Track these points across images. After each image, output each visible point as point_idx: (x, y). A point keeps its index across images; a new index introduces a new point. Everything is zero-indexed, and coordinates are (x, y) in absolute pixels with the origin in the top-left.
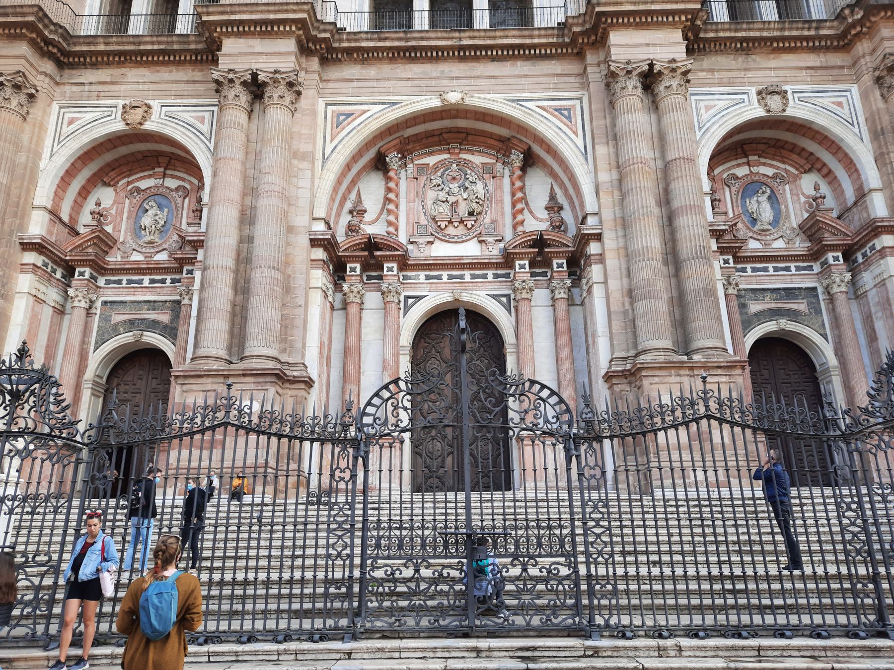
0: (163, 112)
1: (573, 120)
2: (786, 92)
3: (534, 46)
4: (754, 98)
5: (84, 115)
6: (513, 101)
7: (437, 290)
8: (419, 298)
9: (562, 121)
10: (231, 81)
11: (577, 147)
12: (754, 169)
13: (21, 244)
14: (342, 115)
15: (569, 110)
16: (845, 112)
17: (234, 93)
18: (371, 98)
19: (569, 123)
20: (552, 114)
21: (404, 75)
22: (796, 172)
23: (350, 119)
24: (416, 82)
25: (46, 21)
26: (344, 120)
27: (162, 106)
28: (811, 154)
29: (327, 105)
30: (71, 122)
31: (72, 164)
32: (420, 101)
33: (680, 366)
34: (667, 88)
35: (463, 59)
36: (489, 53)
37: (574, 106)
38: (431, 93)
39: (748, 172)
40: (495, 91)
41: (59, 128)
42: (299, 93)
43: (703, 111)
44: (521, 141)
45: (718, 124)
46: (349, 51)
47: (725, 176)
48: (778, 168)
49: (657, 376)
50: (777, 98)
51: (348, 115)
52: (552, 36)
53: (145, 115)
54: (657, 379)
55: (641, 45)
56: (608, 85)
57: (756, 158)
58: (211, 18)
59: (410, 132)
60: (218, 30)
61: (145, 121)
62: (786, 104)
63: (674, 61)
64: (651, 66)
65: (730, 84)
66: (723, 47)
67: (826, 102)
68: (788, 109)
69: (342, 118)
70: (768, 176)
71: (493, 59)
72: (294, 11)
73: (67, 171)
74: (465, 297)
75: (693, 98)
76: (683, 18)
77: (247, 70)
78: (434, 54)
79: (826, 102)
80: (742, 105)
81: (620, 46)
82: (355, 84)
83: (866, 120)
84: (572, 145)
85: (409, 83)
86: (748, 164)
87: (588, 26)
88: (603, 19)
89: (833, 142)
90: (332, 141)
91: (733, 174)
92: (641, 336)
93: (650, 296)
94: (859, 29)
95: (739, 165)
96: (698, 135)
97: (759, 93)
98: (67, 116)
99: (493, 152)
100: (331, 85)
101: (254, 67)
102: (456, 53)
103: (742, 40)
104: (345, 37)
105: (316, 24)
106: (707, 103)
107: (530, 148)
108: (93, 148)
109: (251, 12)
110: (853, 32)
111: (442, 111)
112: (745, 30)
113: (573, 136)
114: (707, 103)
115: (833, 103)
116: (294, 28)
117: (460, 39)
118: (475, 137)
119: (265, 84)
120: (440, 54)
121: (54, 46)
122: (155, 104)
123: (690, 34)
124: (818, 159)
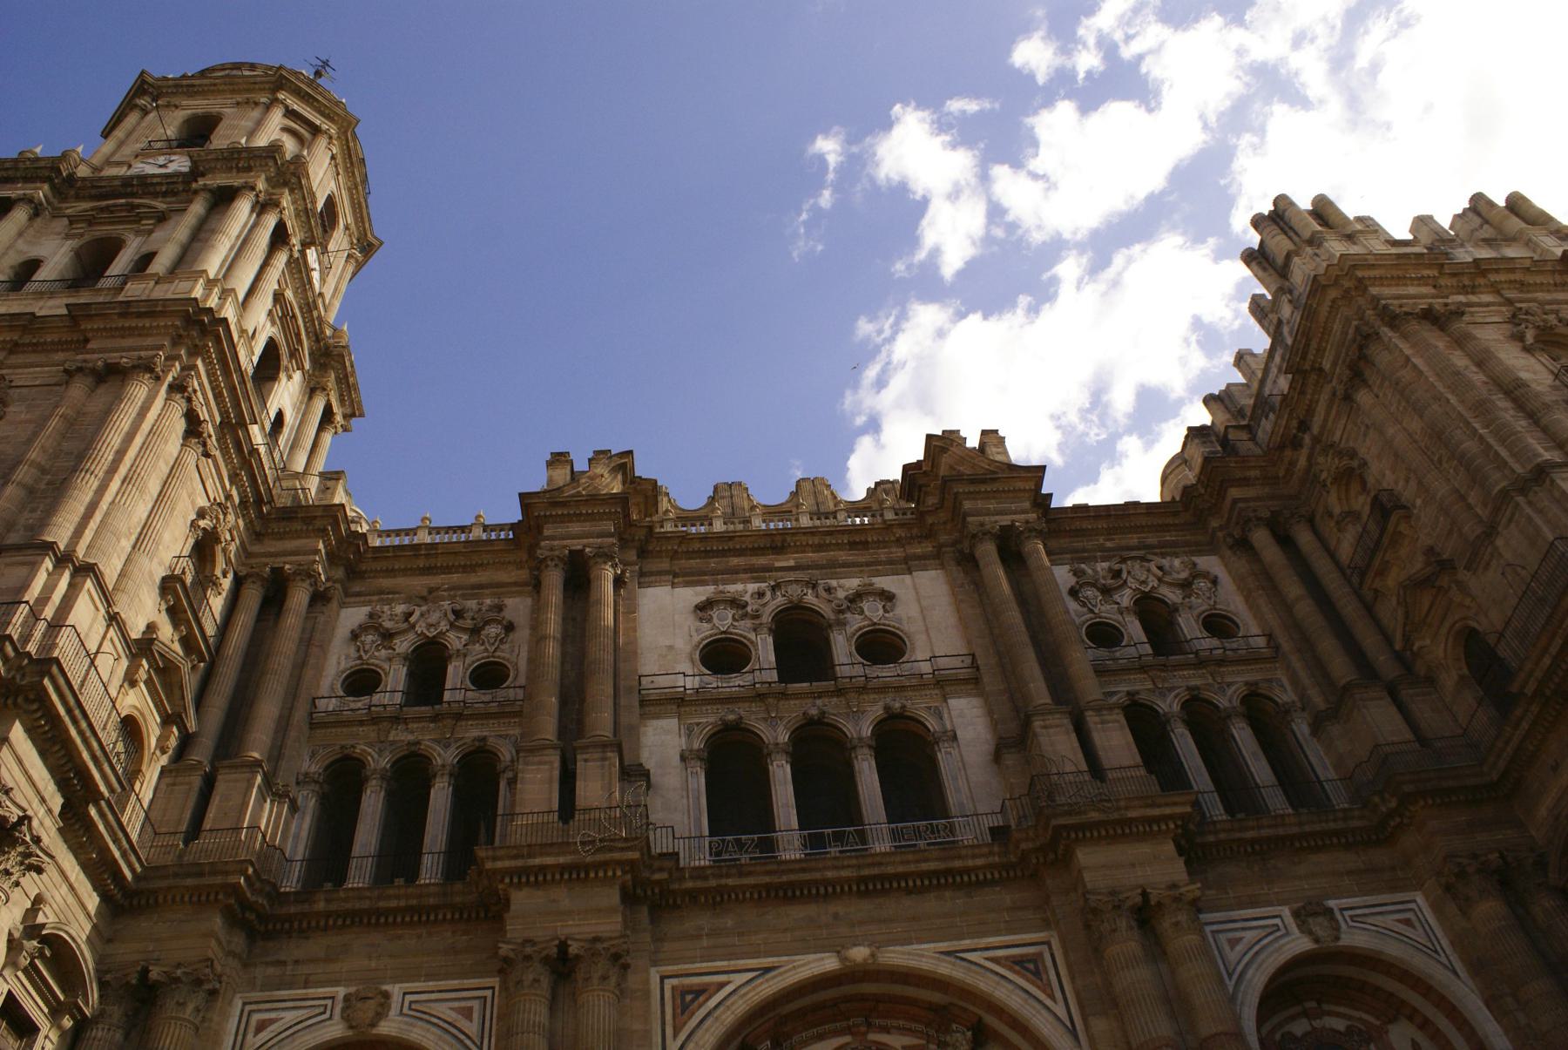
0: (406, 1004)
1: (1044, 977)
2: (1331, 911)
3: (968, 871)
4: (1289, 920)
5: (283, 1014)
6: (948, 953)
9: (1028, 981)
10: (528, 958)
11: (1058, 1019)
12: (1317, 1023)
14: (690, 992)
15: (1036, 959)
16: (1418, 935)
17: (531, 977)
18: (732, 962)
19: (1039, 983)
20: (1010, 969)
22: (1378, 1023)
23: (701, 999)
26: (693, 1001)
27: (405, 994)
28: (1392, 995)
29: (662, 978)
30: (262, 1026)
32: (809, 963)
34: (1177, 924)
35: (865, 894)
36: (903, 884)
37: (1040, 955)
38: (822, 949)
39: (1309, 1028)
40: (920, 941)
41: (240, 1038)
42: (626, 967)
43: (1227, 948)
44: (965, 1010)
45: (1255, 966)
46: (693, 895)
47: (1278, 1036)
48: (1350, 1018)
50: (1320, 919)
51: (701, 992)
52: (991, 853)
53: (380, 1010)
56: (1088, 927)
57: (1313, 1004)
58: (499, 864)
60: (507, 880)
61: (380, 1019)
62: (1337, 929)
63: (1174, 886)
64: (1144, 894)
65: (1254, 903)
66: (1228, 852)
67: (1389, 920)
68: (1343, 936)
69: (689, 998)
70: (1340, 1033)
71: (909, 892)
72: (622, 849)
75: (1208, 929)
76: (1172, 826)
77: (553, 940)
78: (822, 891)
79: (1389, 920)
80: (1278, 934)
82: (705, 942)
83: (1452, 943)
84: (1051, 1019)
86: (1306, 1014)
88: (1065, 834)
89: (1419, 979)
90: (675, 1036)
91: (1289, 1033)
94: (1398, 820)
95: (1293, 1018)
96: (1230, 985)
97: (1296, 914)
98: (256, 1017)
99: (920, 1027)
101: (562, 932)
102: (855, 888)
103: (1253, 842)
106: (1231, 935)
107: (980, 1019)
109: (558, 855)
110: (1392, 824)
112: (1253, 828)
113: (1049, 1002)
114: (1231, 935)
115: (1399, 921)
116: (619, 873)
119: (577, 957)
120: (830, 889)
122: (396, 990)
123: (1183, 842)
124: (1403, 1002)
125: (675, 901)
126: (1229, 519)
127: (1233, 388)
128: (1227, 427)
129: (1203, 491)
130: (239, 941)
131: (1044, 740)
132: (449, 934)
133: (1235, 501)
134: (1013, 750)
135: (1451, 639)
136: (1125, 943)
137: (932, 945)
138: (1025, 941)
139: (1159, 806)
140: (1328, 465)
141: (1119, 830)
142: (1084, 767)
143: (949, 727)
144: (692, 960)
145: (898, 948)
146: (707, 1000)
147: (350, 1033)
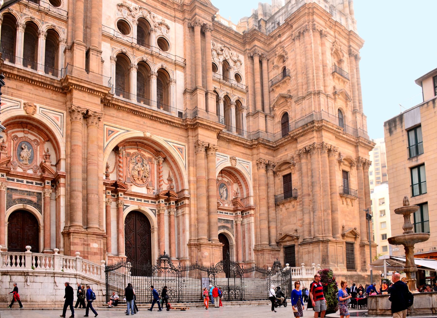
3: (174, 123)
18: (121, 126)
21: (131, 120)
24: (136, 124)
33: (210, 244)
54: (204, 248)
55: (206, 136)
56: (195, 147)
63: (214, 145)
64: (209, 145)
71: (161, 122)
76: (218, 131)
81: (201, 135)
87: (192, 123)
92: (200, 234)
93: (203, 222)
125: (109, 105)
126: (251, 49)
127: (267, 5)
128: (261, 19)
129: (249, 37)
131: (199, 97)
132: (51, 93)
133: (255, 46)
134: (189, 94)
135: (282, 112)
136: (202, 153)
137: (163, 138)
138: (183, 144)
139: (218, 126)
140: (279, 51)
141: (208, 128)
142: (205, 109)
143: (175, 79)
145: (156, 136)
146: (114, 134)
147: (27, 115)
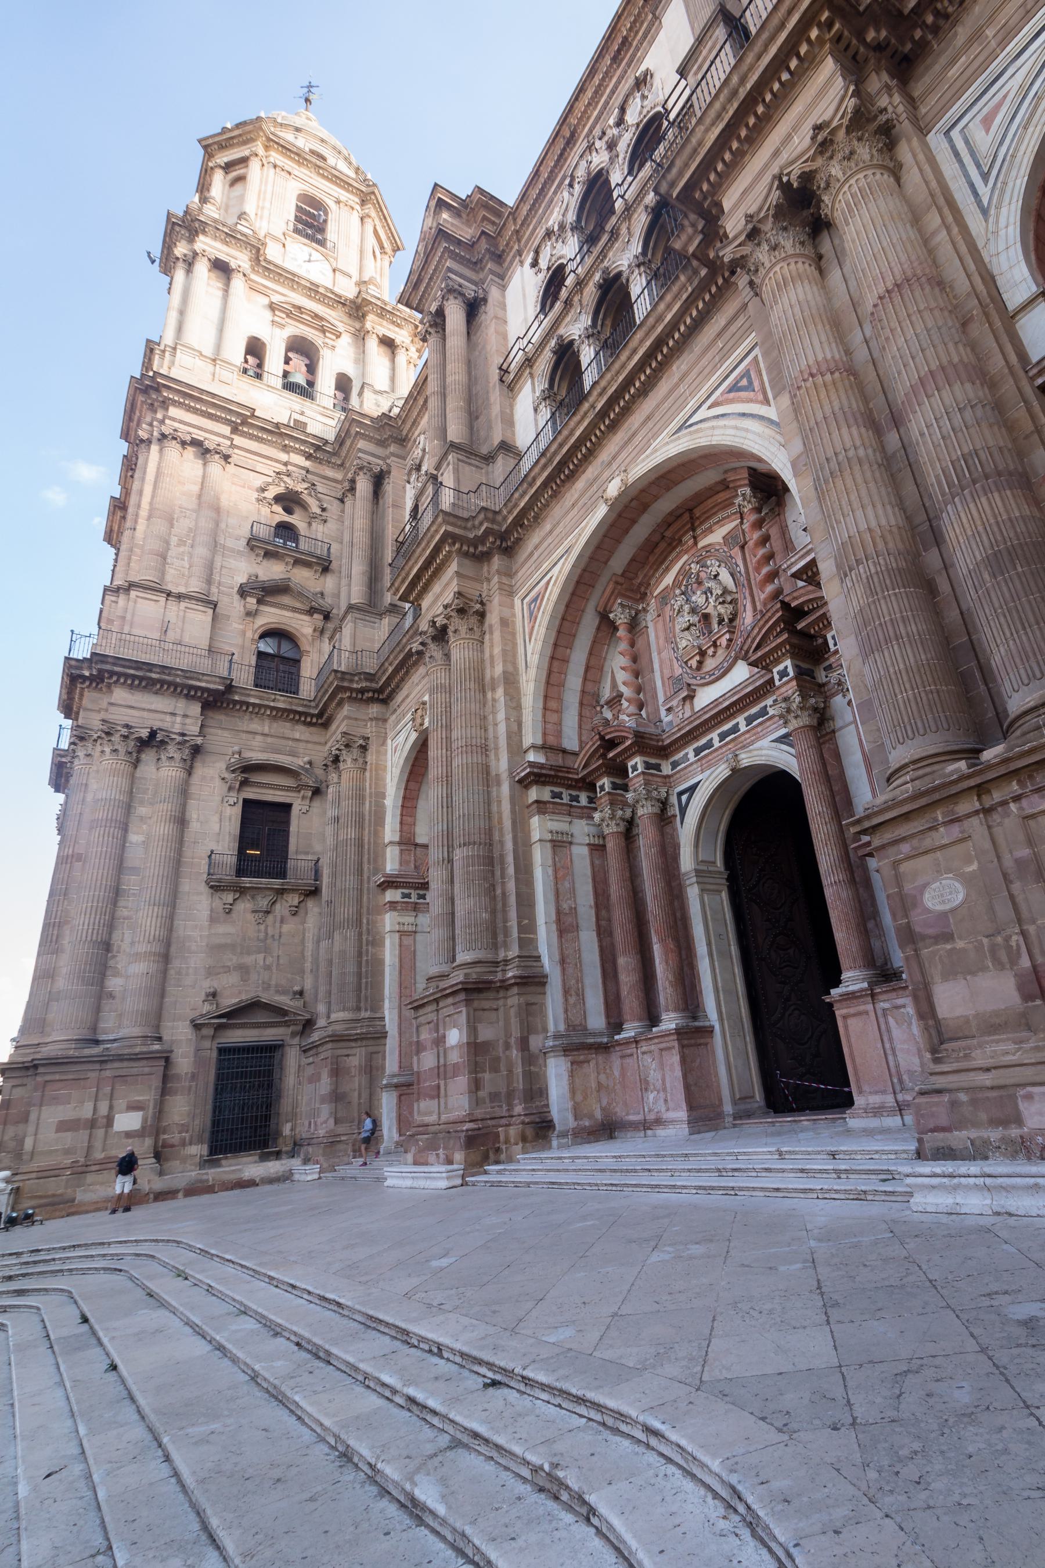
6: (680, 429)
7: (709, 767)
8: (692, 789)
13: (379, 886)
25: (347, 677)
31: (406, 789)
35: (614, 426)
49: (903, 839)
51: (535, 600)
59: (619, 562)
73: (404, 798)
74: (746, 759)
85: (576, 509)
100: (520, 574)
104: (505, 512)
105: (469, 524)
108: (413, 765)
111: (620, 515)
117: (593, 406)
118: (702, 506)
121: (368, 691)
130: (374, 709)
144: (531, 575)
